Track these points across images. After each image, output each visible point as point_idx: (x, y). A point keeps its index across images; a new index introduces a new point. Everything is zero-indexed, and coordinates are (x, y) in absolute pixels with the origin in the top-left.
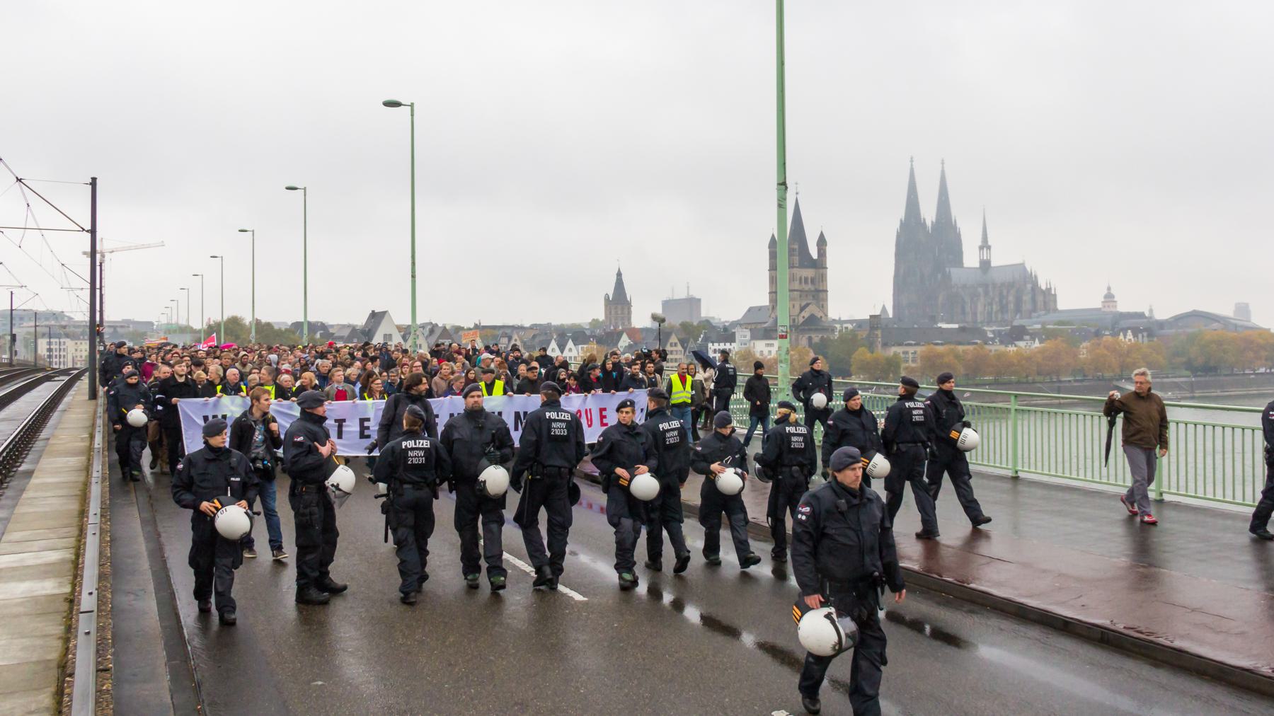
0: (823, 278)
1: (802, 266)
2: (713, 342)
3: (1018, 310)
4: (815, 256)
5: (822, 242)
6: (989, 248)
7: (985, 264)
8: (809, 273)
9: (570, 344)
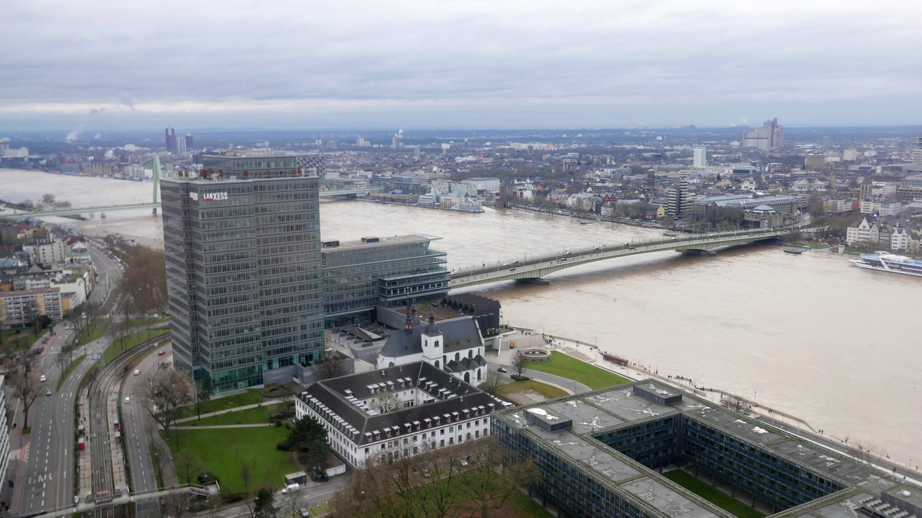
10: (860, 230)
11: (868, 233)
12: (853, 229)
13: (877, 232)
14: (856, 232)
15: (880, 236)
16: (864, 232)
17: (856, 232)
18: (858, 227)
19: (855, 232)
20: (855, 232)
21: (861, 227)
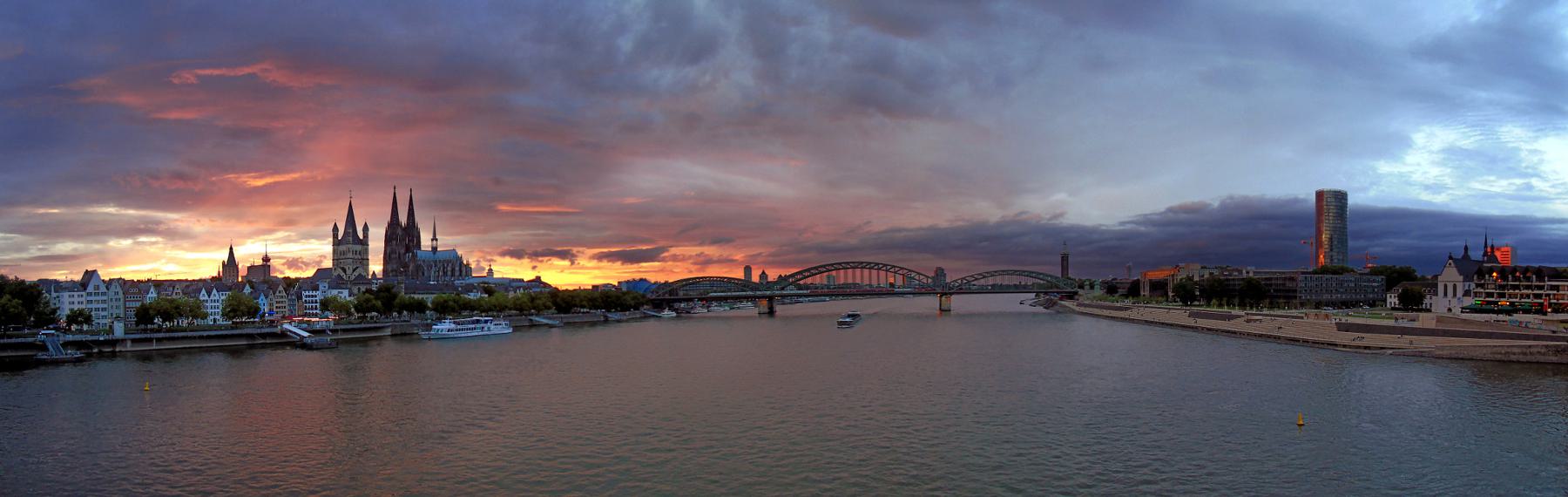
0: (366, 251)
1: (354, 243)
2: (305, 291)
3: (453, 275)
4: (361, 237)
5: (366, 228)
6: (437, 240)
7: (434, 249)
8: (358, 248)
9: (215, 291)
10: (89, 294)
11: (105, 298)
12: (76, 294)
13: (121, 295)
14: (83, 299)
15: (125, 301)
16: (97, 298)
17: (83, 299)
18: (85, 289)
19: (81, 299)
20: (81, 299)
21: (90, 289)
